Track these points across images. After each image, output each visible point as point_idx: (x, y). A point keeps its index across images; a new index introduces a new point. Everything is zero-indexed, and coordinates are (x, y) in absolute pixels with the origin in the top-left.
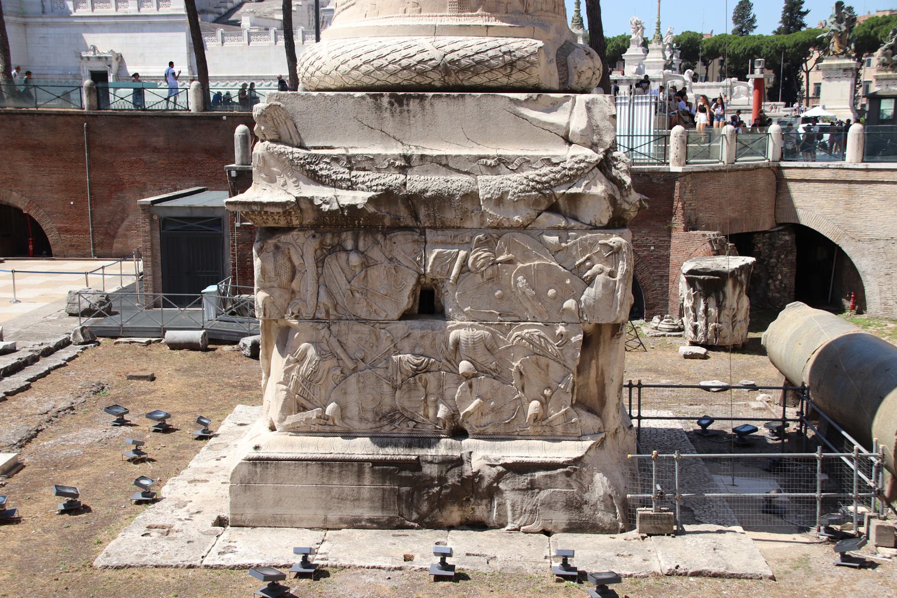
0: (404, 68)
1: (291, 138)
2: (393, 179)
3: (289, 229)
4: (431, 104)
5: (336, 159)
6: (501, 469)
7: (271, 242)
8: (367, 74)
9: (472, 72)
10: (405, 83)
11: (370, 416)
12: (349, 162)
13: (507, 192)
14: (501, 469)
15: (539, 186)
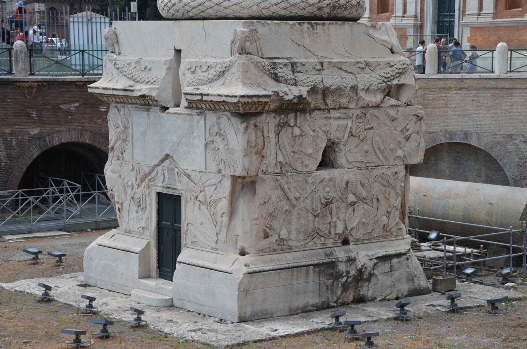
0: (310, 6)
1: (258, 52)
2: (315, 78)
3: (258, 114)
4: (328, 29)
5: (286, 65)
6: (375, 261)
7: (252, 122)
8: (285, 9)
9: (345, 8)
10: (308, 15)
11: (301, 237)
12: (292, 67)
13: (372, 85)
14: (375, 261)
15: (386, 80)
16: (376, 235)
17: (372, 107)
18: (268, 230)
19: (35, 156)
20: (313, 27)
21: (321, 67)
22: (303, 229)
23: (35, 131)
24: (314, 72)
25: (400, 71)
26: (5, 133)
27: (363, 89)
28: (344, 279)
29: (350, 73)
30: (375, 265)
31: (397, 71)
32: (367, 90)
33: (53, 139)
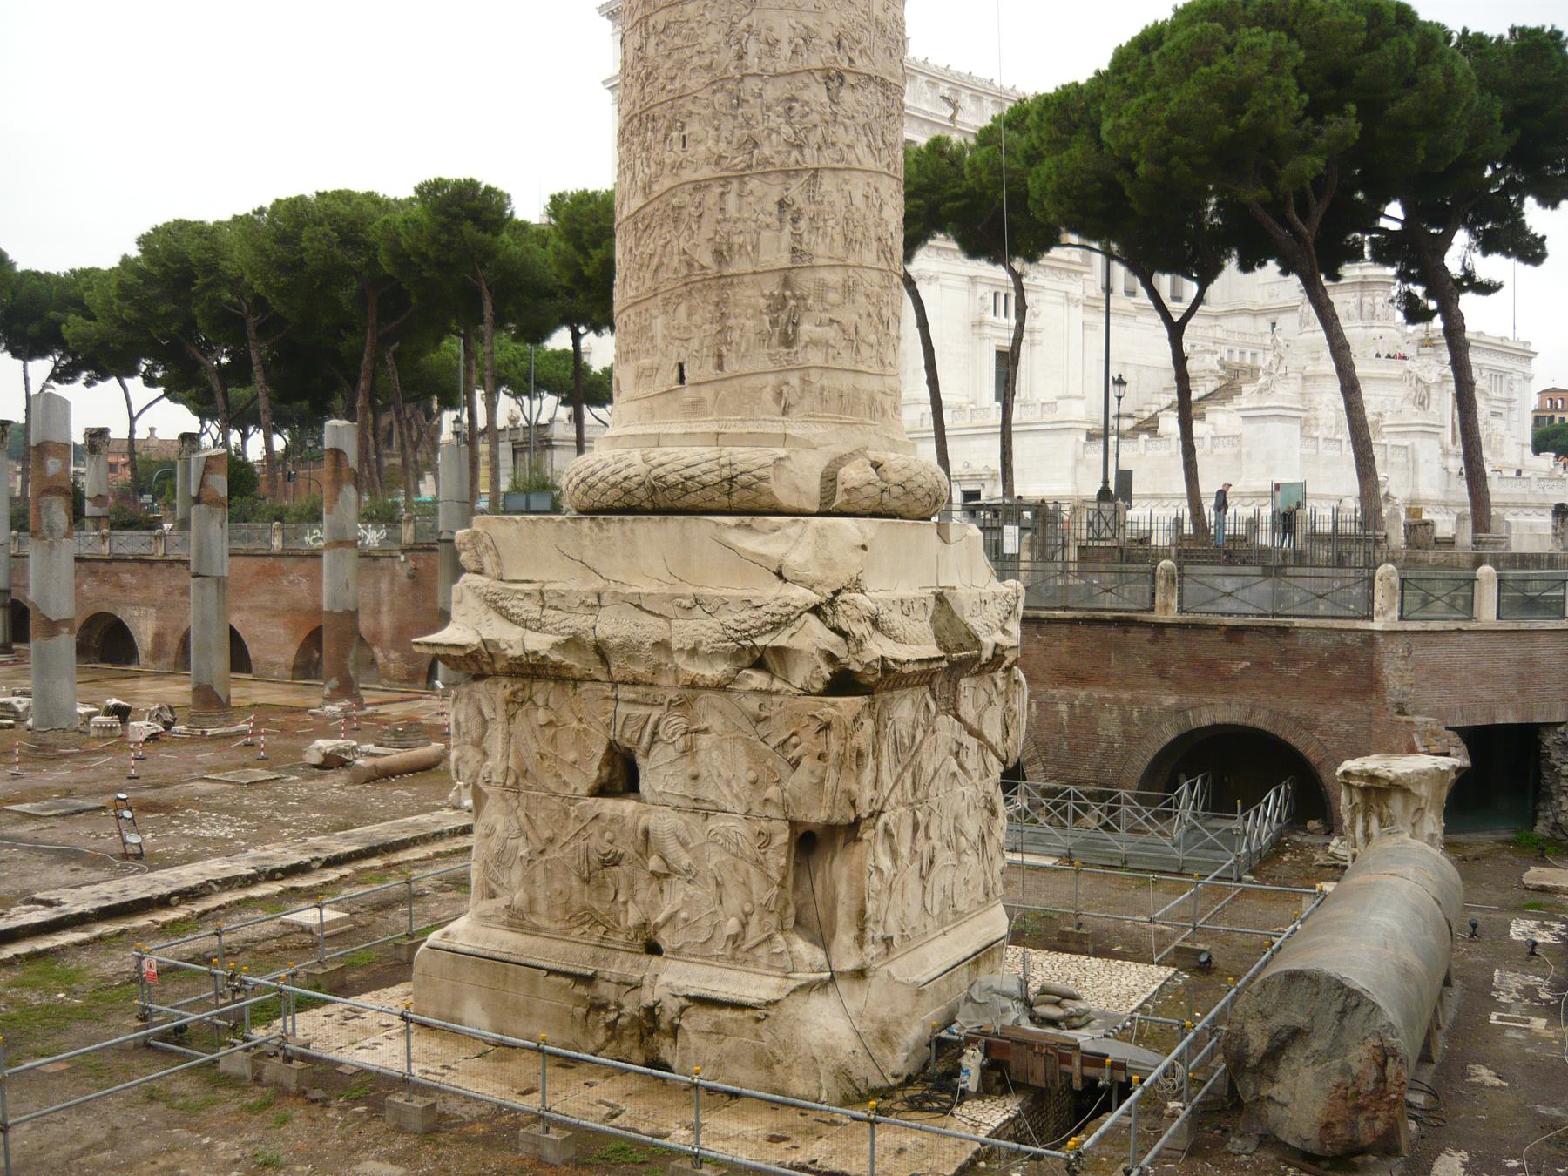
2: (581, 622)
5: (528, 595)
6: (685, 1002)
13: (700, 642)
14: (685, 1002)
16: (715, 952)
17: (707, 688)
18: (494, 886)
19: (1168, 739)
20: (600, 526)
21: (595, 603)
22: (559, 901)
23: (1171, 701)
24: (581, 610)
25: (775, 619)
26: (1121, 699)
27: (681, 650)
28: (612, 1016)
29: (660, 616)
30: (683, 1009)
31: (768, 618)
32: (693, 652)
33: (1200, 716)
